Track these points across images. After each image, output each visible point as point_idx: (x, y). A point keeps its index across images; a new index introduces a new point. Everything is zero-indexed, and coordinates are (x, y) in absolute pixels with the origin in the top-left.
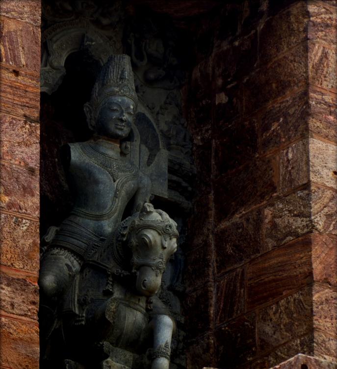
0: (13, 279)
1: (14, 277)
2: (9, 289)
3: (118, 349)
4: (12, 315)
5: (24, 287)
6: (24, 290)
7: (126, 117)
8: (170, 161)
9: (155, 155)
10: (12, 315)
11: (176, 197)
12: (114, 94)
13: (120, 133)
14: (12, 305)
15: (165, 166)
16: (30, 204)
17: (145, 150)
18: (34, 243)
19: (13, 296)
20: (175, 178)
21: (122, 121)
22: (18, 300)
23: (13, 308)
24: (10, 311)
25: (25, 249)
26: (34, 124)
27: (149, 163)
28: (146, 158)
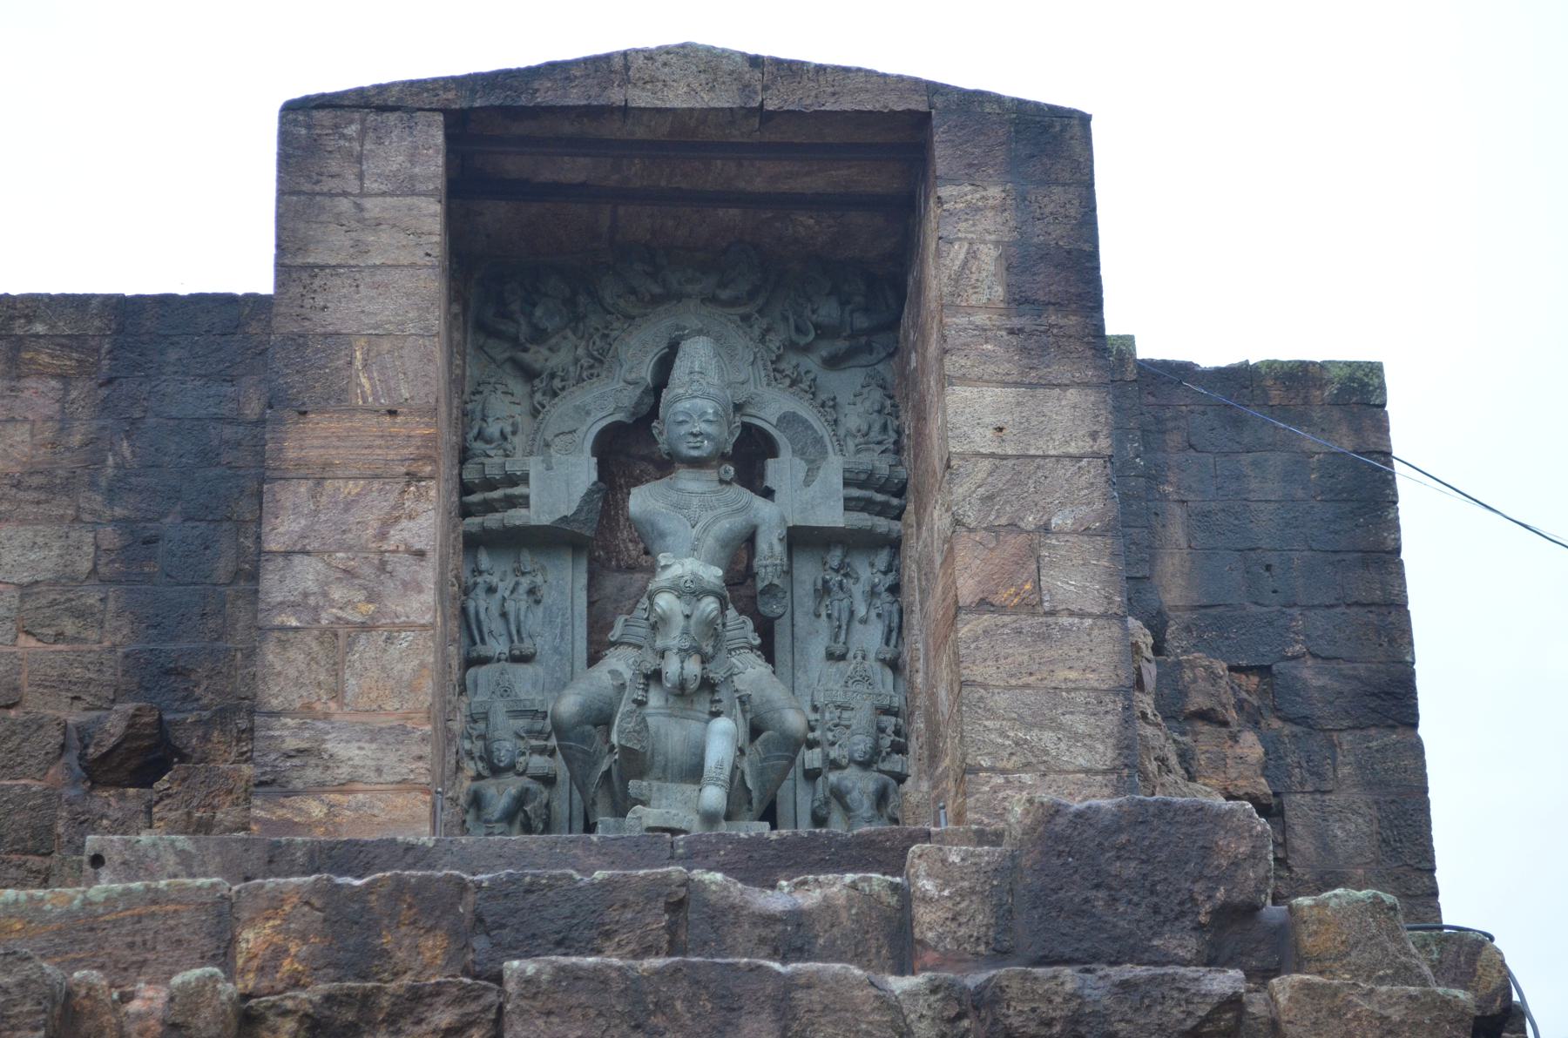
0: (381, 729)
1: (383, 725)
2: (374, 746)
3: (670, 785)
4: (378, 787)
5: (401, 738)
6: (402, 742)
7: (704, 427)
8: (845, 470)
9: (818, 468)
10: (378, 787)
11: (862, 520)
12: (678, 399)
13: (695, 453)
14: (379, 771)
15: (838, 481)
16: (416, 605)
17: (801, 466)
18: (423, 665)
19: (380, 755)
20: (855, 492)
21: (695, 435)
22: (390, 758)
23: (380, 775)
24: (375, 780)
25: (405, 678)
26: (423, 483)
27: (807, 483)
28: (802, 476)
